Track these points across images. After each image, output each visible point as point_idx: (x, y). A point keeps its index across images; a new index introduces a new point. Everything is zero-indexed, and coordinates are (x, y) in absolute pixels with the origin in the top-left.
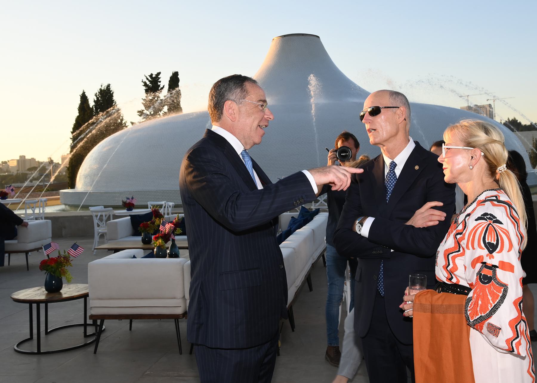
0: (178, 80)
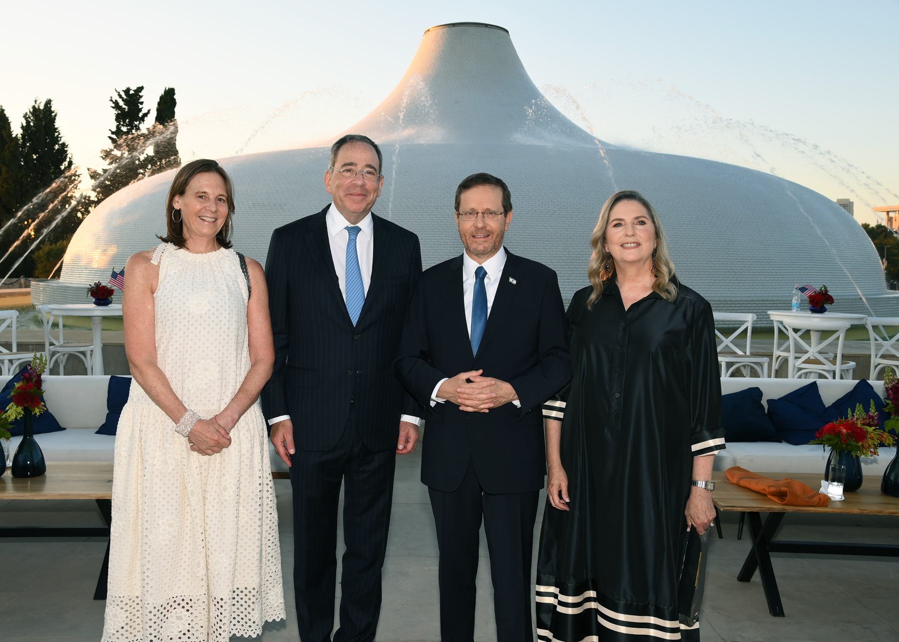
0: (174, 103)
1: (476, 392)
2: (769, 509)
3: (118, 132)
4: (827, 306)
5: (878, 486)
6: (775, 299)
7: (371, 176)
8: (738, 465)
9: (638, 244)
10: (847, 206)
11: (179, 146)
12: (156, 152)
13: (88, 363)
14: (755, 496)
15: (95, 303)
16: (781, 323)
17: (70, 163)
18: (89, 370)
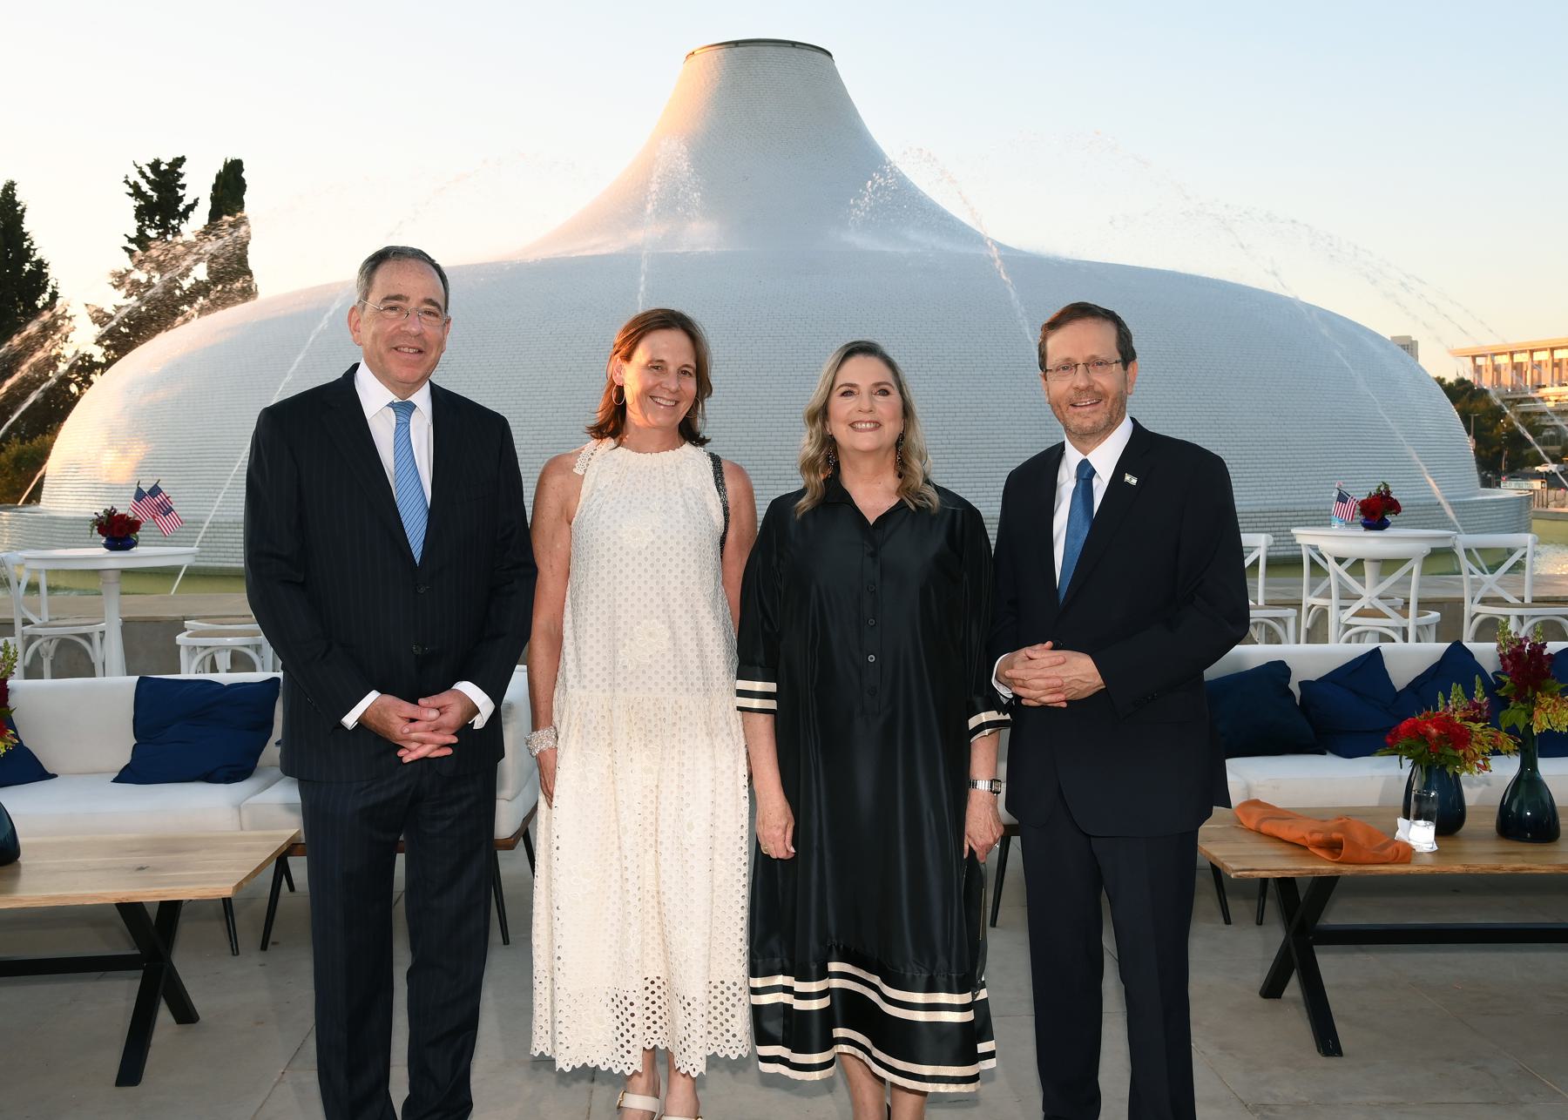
0: (241, 186)
1: (1051, 673)
2: (1313, 871)
3: (141, 240)
4: (1389, 518)
5: (1491, 823)
6: (1298, 507)
7: (432, 318)
8: (1254, 797)
9: (878, 425)
10: (1409, 347)
11: (253, 262)
12: (210, 271)
13: (96, 655)
14: (1288, 850)
15: (106, 546)
16: (1315, 548)
17: (54, 296)
18: (98, 668)
